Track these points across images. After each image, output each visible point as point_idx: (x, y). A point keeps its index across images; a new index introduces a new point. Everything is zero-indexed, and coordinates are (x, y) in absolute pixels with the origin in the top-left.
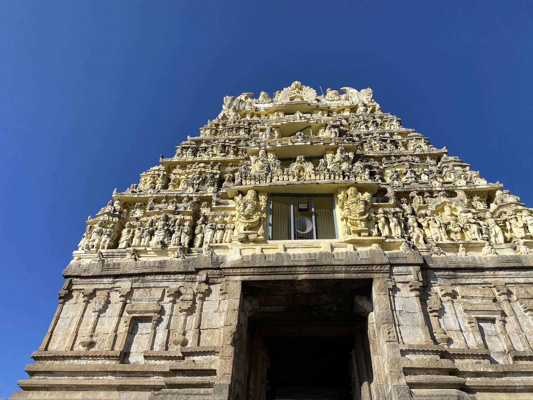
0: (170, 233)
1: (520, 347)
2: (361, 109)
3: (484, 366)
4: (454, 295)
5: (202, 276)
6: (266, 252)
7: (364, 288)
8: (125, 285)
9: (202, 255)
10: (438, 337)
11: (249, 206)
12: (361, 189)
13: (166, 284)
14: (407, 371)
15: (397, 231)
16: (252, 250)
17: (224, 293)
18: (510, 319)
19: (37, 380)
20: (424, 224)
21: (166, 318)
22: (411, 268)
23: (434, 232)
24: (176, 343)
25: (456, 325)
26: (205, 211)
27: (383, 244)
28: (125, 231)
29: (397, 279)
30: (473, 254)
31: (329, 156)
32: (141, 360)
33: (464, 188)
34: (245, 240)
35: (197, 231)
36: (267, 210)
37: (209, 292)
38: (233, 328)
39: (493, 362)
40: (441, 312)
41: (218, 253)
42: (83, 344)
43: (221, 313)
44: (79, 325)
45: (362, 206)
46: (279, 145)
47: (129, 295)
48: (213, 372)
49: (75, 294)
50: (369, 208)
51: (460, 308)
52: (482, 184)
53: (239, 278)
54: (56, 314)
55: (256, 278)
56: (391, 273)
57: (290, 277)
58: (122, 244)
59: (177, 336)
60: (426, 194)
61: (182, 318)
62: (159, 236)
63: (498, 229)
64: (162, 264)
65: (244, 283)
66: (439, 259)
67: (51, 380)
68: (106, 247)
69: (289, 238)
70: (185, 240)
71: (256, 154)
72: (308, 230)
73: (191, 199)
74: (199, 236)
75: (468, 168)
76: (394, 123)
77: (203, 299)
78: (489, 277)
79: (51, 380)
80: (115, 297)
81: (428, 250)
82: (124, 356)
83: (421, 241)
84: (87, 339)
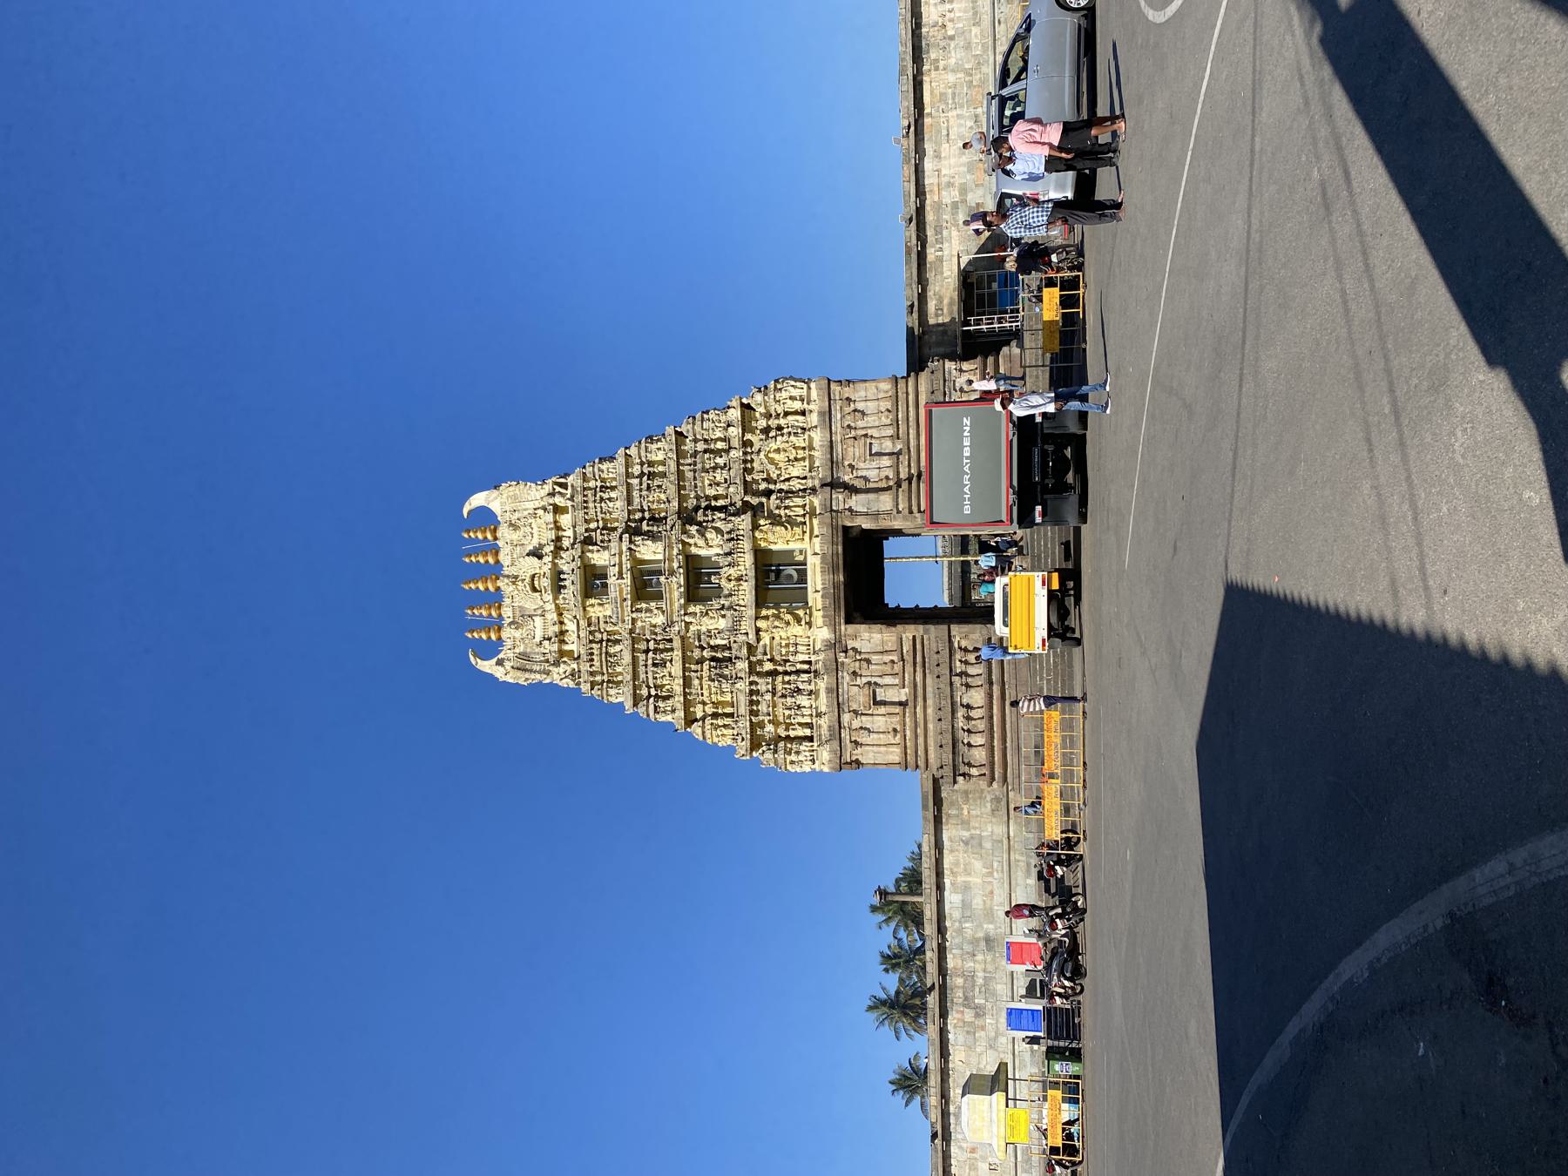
0: (799, 691)
1: (890, 431)
2: (558, 500)
3: (904, 459)
4: (851, 466)
5: (841, 657)
7: (846, 529)
8: (846, 718)
9: (819, 660)
10: (883, 484)
12: (755, 527)
14: (911, 512)
15: (799, 501)
16: (818, 617)
18: (870, 432)
19: (921, 763)
21: (873, 680)
23: (796, 471)
25: (876, 470)
26: (768, 666)
27: (813, 513)
28: (792, 734)
30: (816, 444)
31: (694, 550)
32: (903, 691)
34: (809, 624)
36: (777, 606)
39: (899, 453)
40: (866, 479)
43: (870, 638)
47: (855, 712)
50: (776, 520)
51: (862, 465)
52: (734, 414)
58: (808, 732)
59: (888, 669)
62: (803, 700)
63: (790, 418)
64: (829, 691)
66: (822, 473)
67: (921, 752)
70: (805, 677)
71: (688, 624)
72: (795, 575)
73: (751, 683)
74: (799, 666)
76: (604, 466)
78: (837, 438)
79: (921, 752)
80: (856, 724)
82: (903, 704)
84: (890, 736)
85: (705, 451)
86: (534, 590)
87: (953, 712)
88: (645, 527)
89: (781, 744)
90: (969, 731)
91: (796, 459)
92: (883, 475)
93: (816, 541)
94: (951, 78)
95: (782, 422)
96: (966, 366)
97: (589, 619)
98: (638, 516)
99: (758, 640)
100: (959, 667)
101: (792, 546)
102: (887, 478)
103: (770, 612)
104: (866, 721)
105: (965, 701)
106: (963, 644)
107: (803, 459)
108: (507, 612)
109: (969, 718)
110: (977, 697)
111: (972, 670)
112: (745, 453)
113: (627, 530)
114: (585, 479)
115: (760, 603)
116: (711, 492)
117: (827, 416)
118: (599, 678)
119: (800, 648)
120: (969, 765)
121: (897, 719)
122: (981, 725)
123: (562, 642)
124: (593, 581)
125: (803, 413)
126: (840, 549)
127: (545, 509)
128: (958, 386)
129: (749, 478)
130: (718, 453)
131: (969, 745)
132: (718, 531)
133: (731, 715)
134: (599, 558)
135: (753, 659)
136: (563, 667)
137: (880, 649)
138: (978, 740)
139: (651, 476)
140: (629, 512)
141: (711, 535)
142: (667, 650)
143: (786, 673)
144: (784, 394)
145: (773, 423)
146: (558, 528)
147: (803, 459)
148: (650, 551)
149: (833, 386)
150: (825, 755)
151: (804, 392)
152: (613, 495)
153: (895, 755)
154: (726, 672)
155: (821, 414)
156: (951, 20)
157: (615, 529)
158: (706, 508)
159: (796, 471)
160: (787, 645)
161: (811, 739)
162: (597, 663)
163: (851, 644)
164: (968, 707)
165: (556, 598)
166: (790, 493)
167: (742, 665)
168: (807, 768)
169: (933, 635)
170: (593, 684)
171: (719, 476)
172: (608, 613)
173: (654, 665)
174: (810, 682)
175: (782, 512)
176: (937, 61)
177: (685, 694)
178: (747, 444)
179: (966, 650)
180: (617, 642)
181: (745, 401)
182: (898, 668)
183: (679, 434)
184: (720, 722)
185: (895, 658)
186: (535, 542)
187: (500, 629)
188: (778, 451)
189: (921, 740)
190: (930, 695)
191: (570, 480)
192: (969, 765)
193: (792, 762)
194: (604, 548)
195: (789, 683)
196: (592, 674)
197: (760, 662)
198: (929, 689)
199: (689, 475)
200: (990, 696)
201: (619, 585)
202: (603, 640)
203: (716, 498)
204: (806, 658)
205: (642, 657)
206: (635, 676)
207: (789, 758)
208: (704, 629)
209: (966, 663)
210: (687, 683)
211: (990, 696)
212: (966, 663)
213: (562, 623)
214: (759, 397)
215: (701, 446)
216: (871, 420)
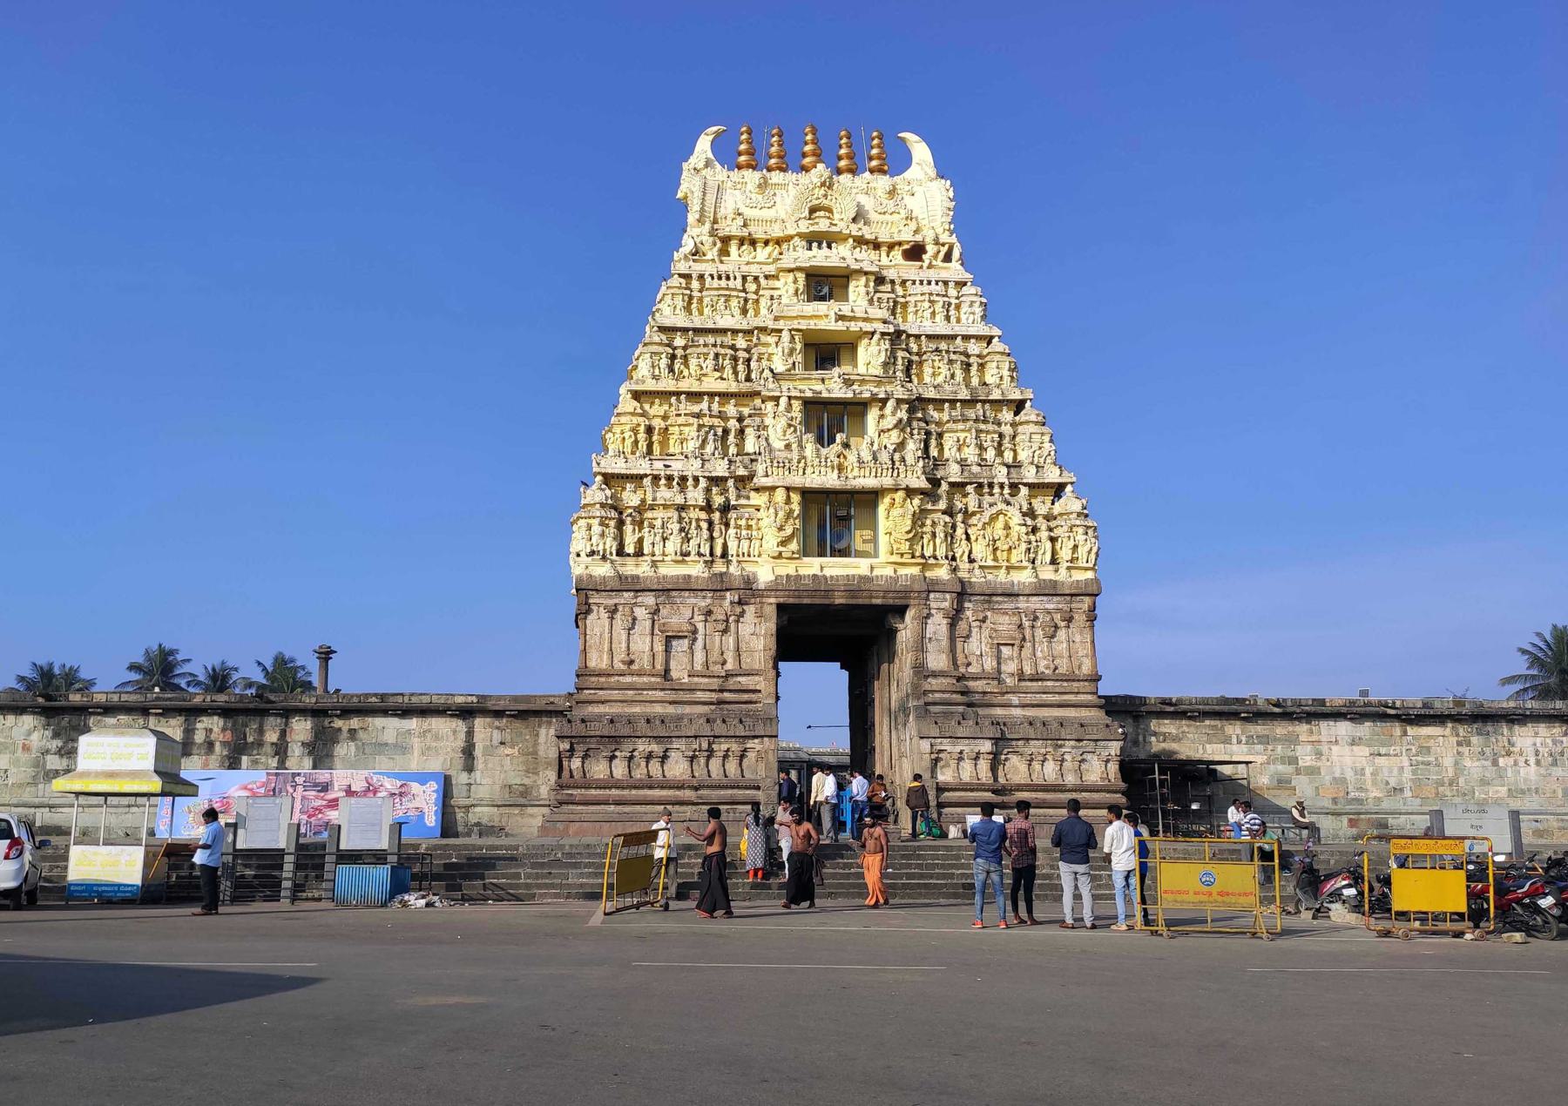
1: (1028, 670)
3: (992, 687)
4: (984, 620)
6: (802, 572)
8: (650, 600)
10: (961, 659)
11: (781, 514)
12: (910, 492)
13: (693, 601)
15: (941, 551)
16: (788, 569)
17: (760, 615)
20: (973, 538)
21: (700, 637)
22: (948, 596)
23: (980, 550)
24: (715, 663)
26: (718, 500)
27: (925, 567)
28: (628, 528)
29: (933, 605)
35: (716, 534)
37: (743, 612)
39: (1000, 681)
41: (749, 568)
42: (623, 662)
43: (757, 633)
45: (909, 522)
46: (809, 394)
47: (657, 611)
49: (594, 608)
50: (919, 517)
51: (986, 633)
52: (1053, 475)
53: (773, 600)
55: (791, 601)
56: (927, 599)
57: (826, 602)
58: (630, 549)
59: (715, 656)
61: (717, 639)
62: (673, 545)
63: (1049, 545)
70: (705, 549)
77: (737, 621)
78: (1022, 603)
80: (640, 612)
81: (970, 571)
83: (965, 558)
85: (1001, 436)
86: (813, 210)
87: (658, 739)
88: (900, 354)
89: (614, 514)
90: (631, 758)
91: (995, 550)
92: (973, 659)
93: (889, 571)
94: (1448, 762)
95: (1044, 534)
96: (1113, 768)
97: (776, 277)
98: (914, 347)
99: (757, 490)
100: (721, 747)
101: (883, 540)
102: (969, 664)
103: (796, 508)
104: (644, 624)
105: (672, 754)
106: (751, 755)
107: (996, 559)
108: (776, 177)
109: (649, 757)
110: (677, 768)
111: (715, 764)
112: (1002, 486)
113: (898, 333)
115: (808, 494)
116: (949, 440)
117: (1048, 590)
118: (695, 284)
119: (745, 544)
120: (585, 757)
121: (647, 666)
122: (639, 773)
123: (742, 242)
124: (824, 284)
125: (1054, 561)
126: (878, 601)
127: (916, 232)
128: (1089, 757)
129: (970, 489)
130: (1000, 453)
131: (613, 758)
132: (901, 446)
133: (650, 451)
134: (858, 290)
135: (731, 483)
136: (707, 240)
137: (743, 646)
138: (619, 769)
139: (967, 367)
140: (918, 337)
141: (895, 437)
142: (736, 373)
143: (711, 523)
144: (1080, 538)
145: (1042, 524)
146: (891, 247)
147: (996, 559)
148: (870, 357)
149: (1087, 599)
150: (602, 570)
152: (939, 318)
153: (597, 661)
154: (709, 448)
155: (1054, 583)
156: (1516, 763)
157: (894, 313)
158: (928, 433)
159: (980, 550)
160: (749, 527)
161: (621, 552)
162: (716, 283)
163: (750, 610)
164: (664, 758)
165: (800, 235)
166: (950, 536)
167: (720, 468)
170: (687, 277)
171: (970, 453)
172: (785, 300)
173: (717, 355)
174: (700, 554)
175: (928, 529)
176: (1469, 744)
177: (678, 394)
179: (742, 757)
180: (744, 312)
181: (1069, 488)
182: (716, 669)
183: (1019, 406)
184: (642, 436)
185: (729, 666)
186: (873, 216)
187: (754, 168)
188: (1007, 527)
189: (615, 694)
190: (680, 710)
191: (955, 265)
192: (585, 757)
193: (589, 528)
194: (871, 302)
195: (699, 527)
196: (701, 277)
197: (724, 491)
198: (687, 709)
199: (971, 414)
200: (680, 786)
201: (824, 316)
202: (748, 291)
203: (940, 446)
204: (732, 549)
205: (728, 339)
206: (697, 331)
207: (595, 522)
208: (768, 421)
209: (725, 757)
210: (695, 396)
211: (680, 786)
212: (725, 757)
213: (766, 243)
214: (1076, 506)
215: (1007, 430)
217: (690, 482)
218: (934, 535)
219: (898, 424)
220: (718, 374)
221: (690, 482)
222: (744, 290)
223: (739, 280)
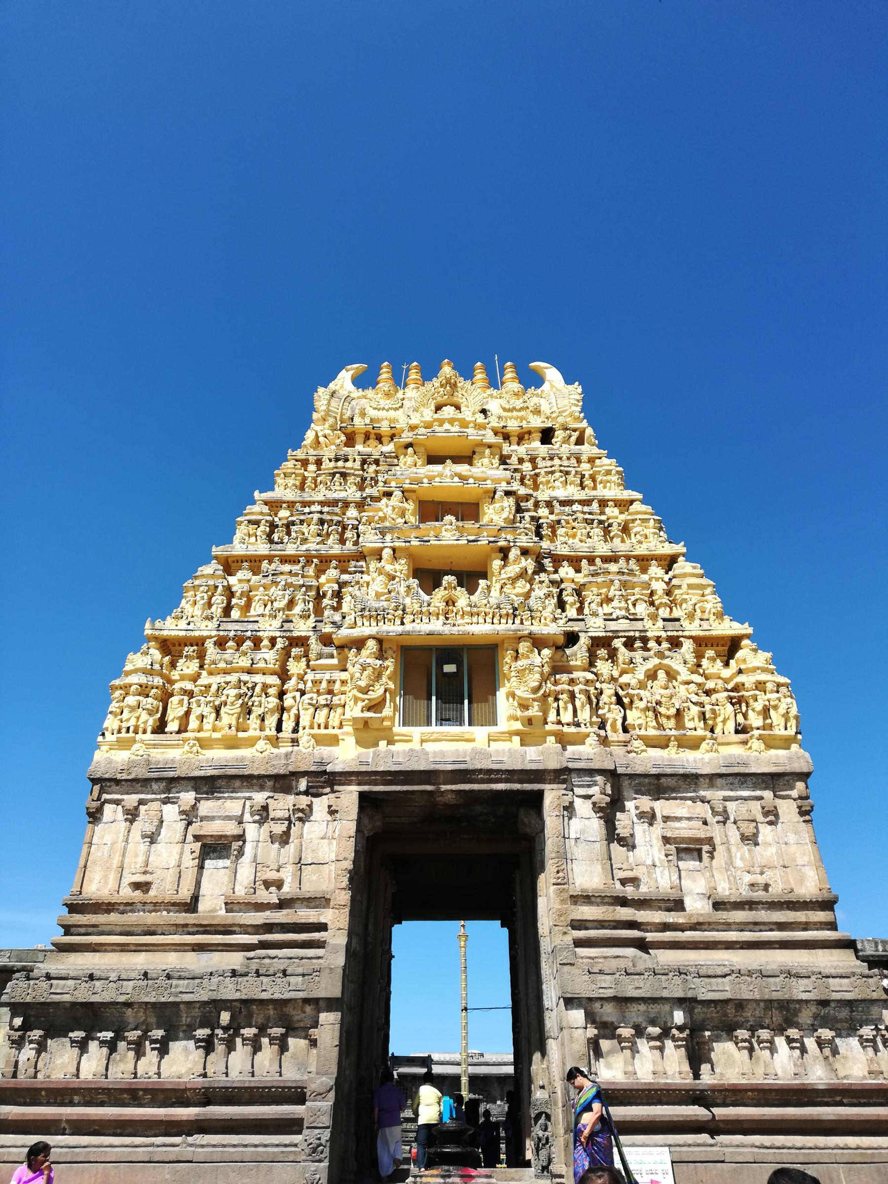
14: (577, 925)
33: (694, 634)
38: (349, 865)
44: (124, 855)
48: (323, 927)
54: (87, 838)
58: (173, 726)
60: (638, 644)
65: (362, 795)
68: (149, 729)
69: (429, 723)
75: (709, 590)
89: (158, 681)
107: (660, 727)
114: (591, 460)
118: (312, 467)
147: (660, 727)
151: (779, 731)
162: (332, 464)
167: (302, 628)
168: (111, 723)
169: (325, 968)
170: (305, 463)
178: (675, 643)
181: (745, 642)
183: (669, 562)
185: (286, 888)
216: (741, 854)
217: (266, 642)
218: (572, 696)
219: (523, 574)
220: (319, 539)
221: (266, 642)
222: (363, 470)
223: (357, 465)
